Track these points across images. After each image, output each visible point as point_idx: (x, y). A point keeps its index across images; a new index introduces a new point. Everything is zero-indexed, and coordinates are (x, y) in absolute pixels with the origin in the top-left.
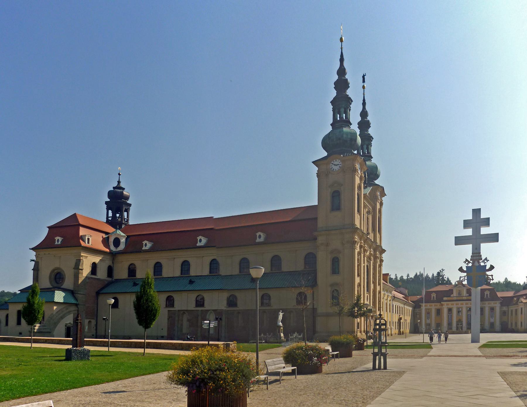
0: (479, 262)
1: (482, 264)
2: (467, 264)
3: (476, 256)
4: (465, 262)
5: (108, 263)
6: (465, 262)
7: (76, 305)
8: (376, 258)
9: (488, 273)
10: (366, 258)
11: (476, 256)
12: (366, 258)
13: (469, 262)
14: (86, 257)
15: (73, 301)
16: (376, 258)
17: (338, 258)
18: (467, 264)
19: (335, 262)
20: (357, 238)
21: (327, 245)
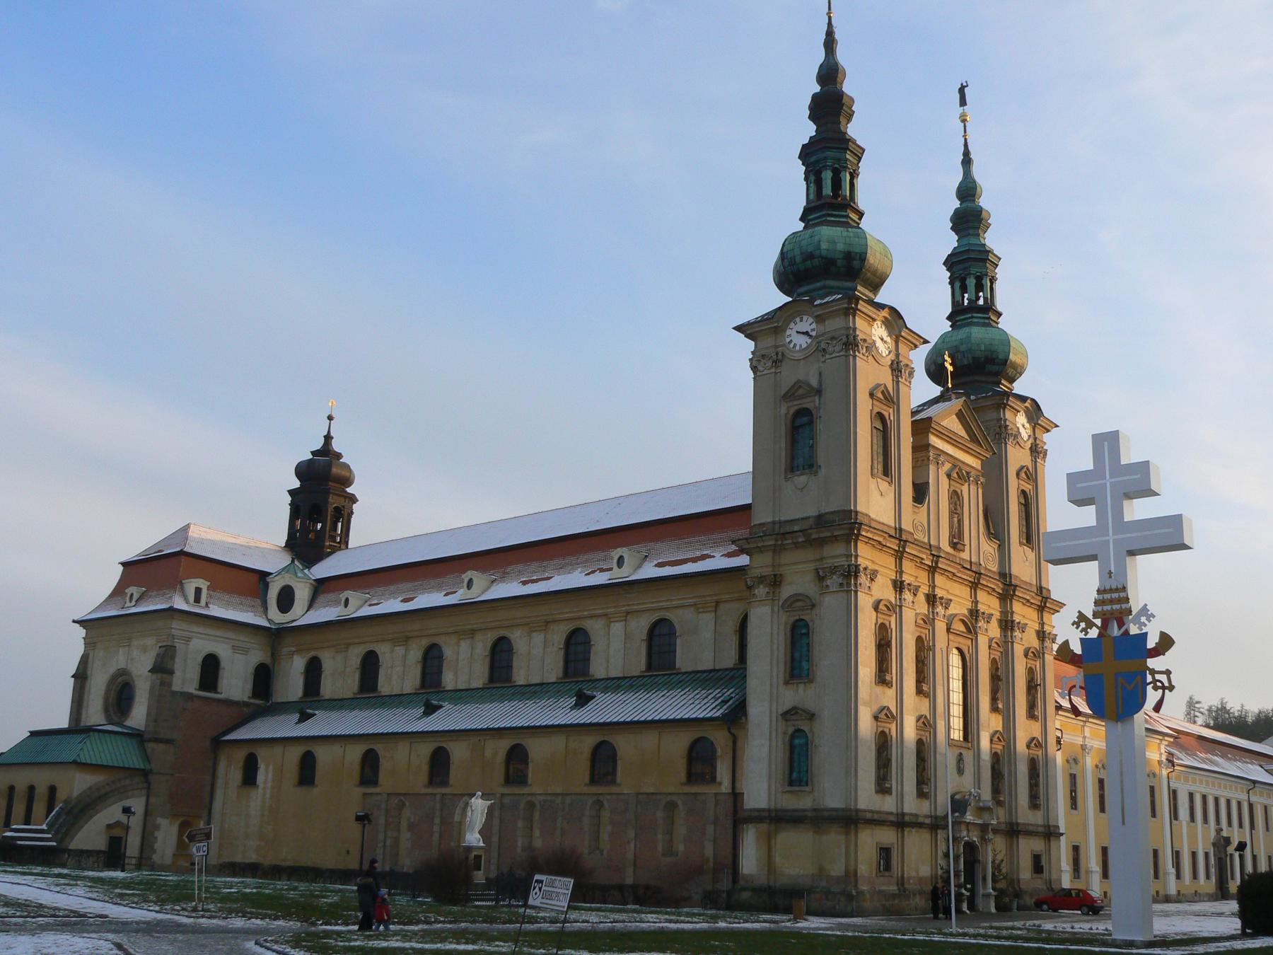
0: (1121, 624)
1: (1134, 630)
2: (1085, 631)
3: (1112, 601)
4: (1076, 624)
5: (257, 655)
6: (1076, 624)
7: (145, 774)
8: (1007, 625)
9: (1152, 663)
10: (940, 626)
11: (1112, 601)
12: (940, 626)
13: (1090, 625)
14: (188, 639)
15: (135, 761)
16: (1007, 625)
17: (807, 626)
18: (1085, 631)
19: (799, 639)
20: (866, 555)
21: (775, 582)
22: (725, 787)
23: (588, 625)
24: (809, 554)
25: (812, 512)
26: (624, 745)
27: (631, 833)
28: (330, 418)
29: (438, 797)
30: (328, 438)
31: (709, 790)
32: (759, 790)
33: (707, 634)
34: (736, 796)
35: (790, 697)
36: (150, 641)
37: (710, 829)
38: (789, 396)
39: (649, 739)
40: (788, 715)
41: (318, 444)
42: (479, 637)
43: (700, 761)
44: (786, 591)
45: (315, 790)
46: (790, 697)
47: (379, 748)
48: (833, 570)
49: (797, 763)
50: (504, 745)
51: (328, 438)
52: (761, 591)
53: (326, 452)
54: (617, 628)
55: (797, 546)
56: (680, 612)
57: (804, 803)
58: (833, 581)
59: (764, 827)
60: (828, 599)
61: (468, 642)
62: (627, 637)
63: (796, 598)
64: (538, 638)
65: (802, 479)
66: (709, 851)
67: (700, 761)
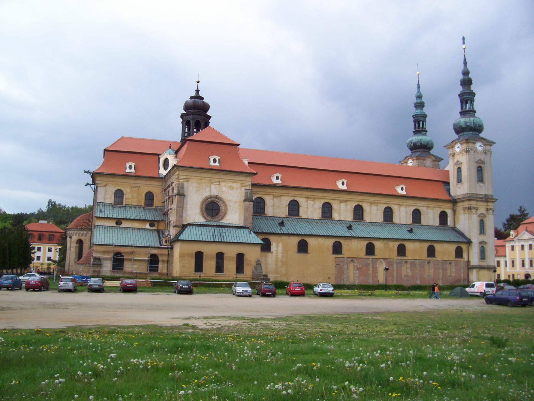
22: (466, 259)
23: (393, 207)
24: (484, 204)
25: (483, 193)
26: (437, 247)
27: (441, 271)
28: (198, 82)
29: (370, 260)
30: (197, 91)
31: (461, 260)
32: (475, 260)
33: (431, 216)
34: (468, 262)
35: (482, 238)
36: (235, 185)
37: (462, 270)
38: (477, 162)
39: (446, 246)
40: (480, 243)
41: (194, 94)
42: (348, 203)
43: (459, 253)
44: (479, 212)
45: (308, 256)
46: (482, 238)
47: (342, 241)
48: (491, 209)
49: (483, 255)
50: (397, 244)
51: (197, 91)
52: (474, 211)
53: (197, 97)
54: (403, 209)
55: (482, 201)
56: (422, 208)
57: (484, 264)
58: (491, 212)
59: (478, 269)
60: (489, 216)
61: (344, 204)
62: (406, 212)
63: (482, 214)
64: (374, 207)
65: (481, 184)
66: (462, 275)
67: (459, 253)
